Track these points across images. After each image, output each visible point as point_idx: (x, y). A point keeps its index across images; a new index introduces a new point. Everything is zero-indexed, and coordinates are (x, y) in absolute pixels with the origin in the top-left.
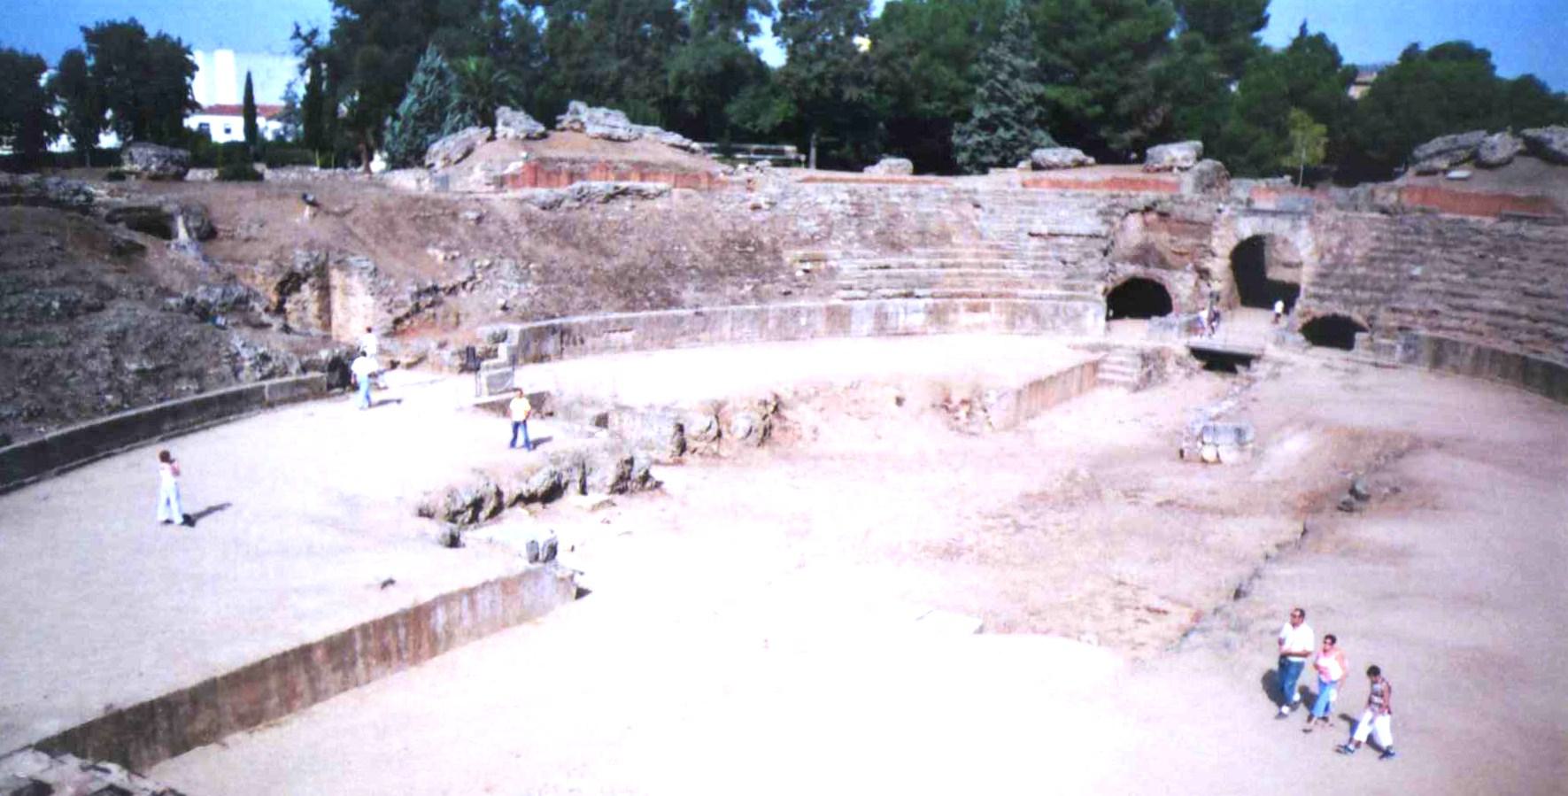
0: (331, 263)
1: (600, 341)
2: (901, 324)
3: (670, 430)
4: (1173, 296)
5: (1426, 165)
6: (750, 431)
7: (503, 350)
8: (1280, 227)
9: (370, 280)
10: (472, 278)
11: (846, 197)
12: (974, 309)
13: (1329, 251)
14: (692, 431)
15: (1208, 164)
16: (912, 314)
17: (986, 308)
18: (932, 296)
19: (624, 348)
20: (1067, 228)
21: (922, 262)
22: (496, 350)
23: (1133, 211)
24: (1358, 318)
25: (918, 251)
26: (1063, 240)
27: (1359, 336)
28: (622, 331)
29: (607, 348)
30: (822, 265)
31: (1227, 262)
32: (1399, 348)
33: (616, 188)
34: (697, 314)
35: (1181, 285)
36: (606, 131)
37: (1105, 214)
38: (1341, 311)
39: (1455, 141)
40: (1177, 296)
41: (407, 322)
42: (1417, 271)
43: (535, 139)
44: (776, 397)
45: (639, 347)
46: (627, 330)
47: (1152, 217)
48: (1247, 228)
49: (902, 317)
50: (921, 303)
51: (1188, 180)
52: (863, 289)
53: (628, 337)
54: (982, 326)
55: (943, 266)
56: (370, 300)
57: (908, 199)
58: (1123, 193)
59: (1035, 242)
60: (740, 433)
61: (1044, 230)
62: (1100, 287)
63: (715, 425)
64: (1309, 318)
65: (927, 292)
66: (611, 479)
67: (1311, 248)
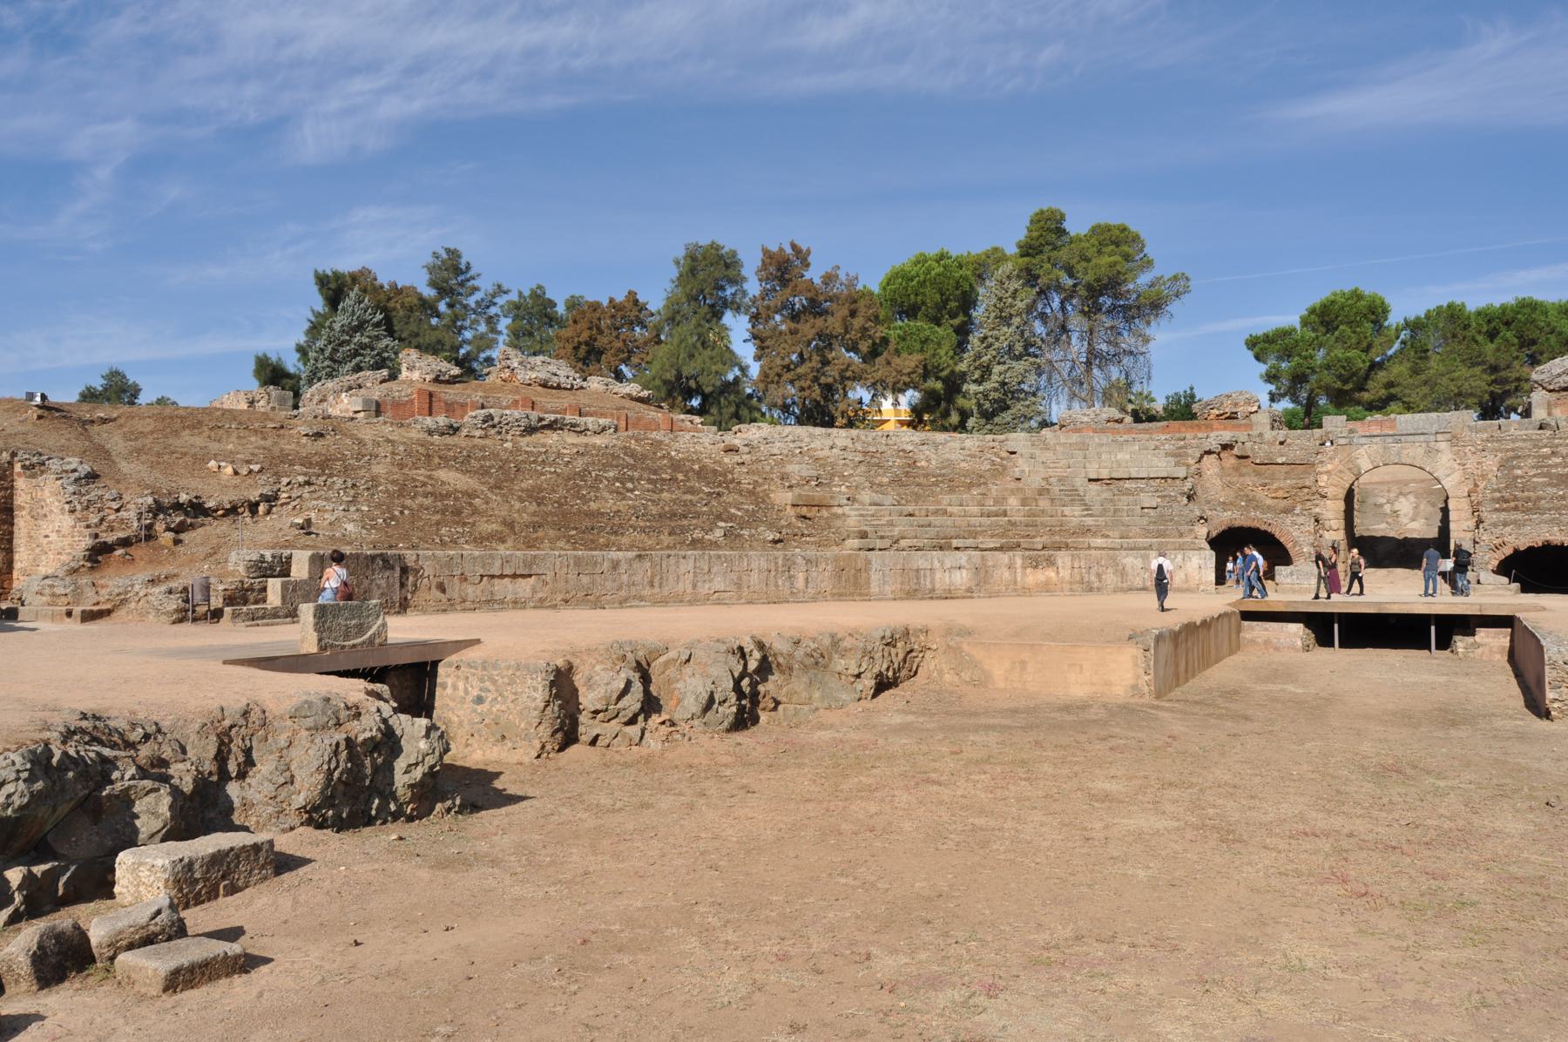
0: (18, 468)
1: (471, 591)
2: (937, 586)
3: (536, 692)
4: (1289, 546)
6: (711, 700)
9: (71, 489)
10: (271, 499)
13: (1483, 476)
14: (589, 699)
15: (1285, 404)
16: (953, 570)
17: (1051, 562)
18: (976, 548)
19: (517, 604)
21: (955, 509)
22: (264, 589)
23: (1209, 452)
25: (946, 499)
26: (1128, 484)
28: (515, 576)
29: (490, 603)
30: (825, 513)
33: (541, 419)
34: (640, 556)
35: (1294, 532)
36: (543, 375)
37: (1178, 455)
40: (1296, 543)
41: (119, 552)
43: (448, 382)
44: (761, 646)
45: (541, 604)
46: (523, 576)
47: (1229, 460)
49: (938, 575)
50: (962, 557)
51: (1263, 419)
52: (882, 537)
53: (524, 587)
54: (1046, 588)
56: (68, 520)
58: (1189, 436)
59: (1094, 487)
60: (692, 705)
61: (1104, 474)
62: (1202, 531)
63: (637, 687)
64: (1508, 551)
65: (969, 542)
66: (308, 787)
67: (1457, 476)
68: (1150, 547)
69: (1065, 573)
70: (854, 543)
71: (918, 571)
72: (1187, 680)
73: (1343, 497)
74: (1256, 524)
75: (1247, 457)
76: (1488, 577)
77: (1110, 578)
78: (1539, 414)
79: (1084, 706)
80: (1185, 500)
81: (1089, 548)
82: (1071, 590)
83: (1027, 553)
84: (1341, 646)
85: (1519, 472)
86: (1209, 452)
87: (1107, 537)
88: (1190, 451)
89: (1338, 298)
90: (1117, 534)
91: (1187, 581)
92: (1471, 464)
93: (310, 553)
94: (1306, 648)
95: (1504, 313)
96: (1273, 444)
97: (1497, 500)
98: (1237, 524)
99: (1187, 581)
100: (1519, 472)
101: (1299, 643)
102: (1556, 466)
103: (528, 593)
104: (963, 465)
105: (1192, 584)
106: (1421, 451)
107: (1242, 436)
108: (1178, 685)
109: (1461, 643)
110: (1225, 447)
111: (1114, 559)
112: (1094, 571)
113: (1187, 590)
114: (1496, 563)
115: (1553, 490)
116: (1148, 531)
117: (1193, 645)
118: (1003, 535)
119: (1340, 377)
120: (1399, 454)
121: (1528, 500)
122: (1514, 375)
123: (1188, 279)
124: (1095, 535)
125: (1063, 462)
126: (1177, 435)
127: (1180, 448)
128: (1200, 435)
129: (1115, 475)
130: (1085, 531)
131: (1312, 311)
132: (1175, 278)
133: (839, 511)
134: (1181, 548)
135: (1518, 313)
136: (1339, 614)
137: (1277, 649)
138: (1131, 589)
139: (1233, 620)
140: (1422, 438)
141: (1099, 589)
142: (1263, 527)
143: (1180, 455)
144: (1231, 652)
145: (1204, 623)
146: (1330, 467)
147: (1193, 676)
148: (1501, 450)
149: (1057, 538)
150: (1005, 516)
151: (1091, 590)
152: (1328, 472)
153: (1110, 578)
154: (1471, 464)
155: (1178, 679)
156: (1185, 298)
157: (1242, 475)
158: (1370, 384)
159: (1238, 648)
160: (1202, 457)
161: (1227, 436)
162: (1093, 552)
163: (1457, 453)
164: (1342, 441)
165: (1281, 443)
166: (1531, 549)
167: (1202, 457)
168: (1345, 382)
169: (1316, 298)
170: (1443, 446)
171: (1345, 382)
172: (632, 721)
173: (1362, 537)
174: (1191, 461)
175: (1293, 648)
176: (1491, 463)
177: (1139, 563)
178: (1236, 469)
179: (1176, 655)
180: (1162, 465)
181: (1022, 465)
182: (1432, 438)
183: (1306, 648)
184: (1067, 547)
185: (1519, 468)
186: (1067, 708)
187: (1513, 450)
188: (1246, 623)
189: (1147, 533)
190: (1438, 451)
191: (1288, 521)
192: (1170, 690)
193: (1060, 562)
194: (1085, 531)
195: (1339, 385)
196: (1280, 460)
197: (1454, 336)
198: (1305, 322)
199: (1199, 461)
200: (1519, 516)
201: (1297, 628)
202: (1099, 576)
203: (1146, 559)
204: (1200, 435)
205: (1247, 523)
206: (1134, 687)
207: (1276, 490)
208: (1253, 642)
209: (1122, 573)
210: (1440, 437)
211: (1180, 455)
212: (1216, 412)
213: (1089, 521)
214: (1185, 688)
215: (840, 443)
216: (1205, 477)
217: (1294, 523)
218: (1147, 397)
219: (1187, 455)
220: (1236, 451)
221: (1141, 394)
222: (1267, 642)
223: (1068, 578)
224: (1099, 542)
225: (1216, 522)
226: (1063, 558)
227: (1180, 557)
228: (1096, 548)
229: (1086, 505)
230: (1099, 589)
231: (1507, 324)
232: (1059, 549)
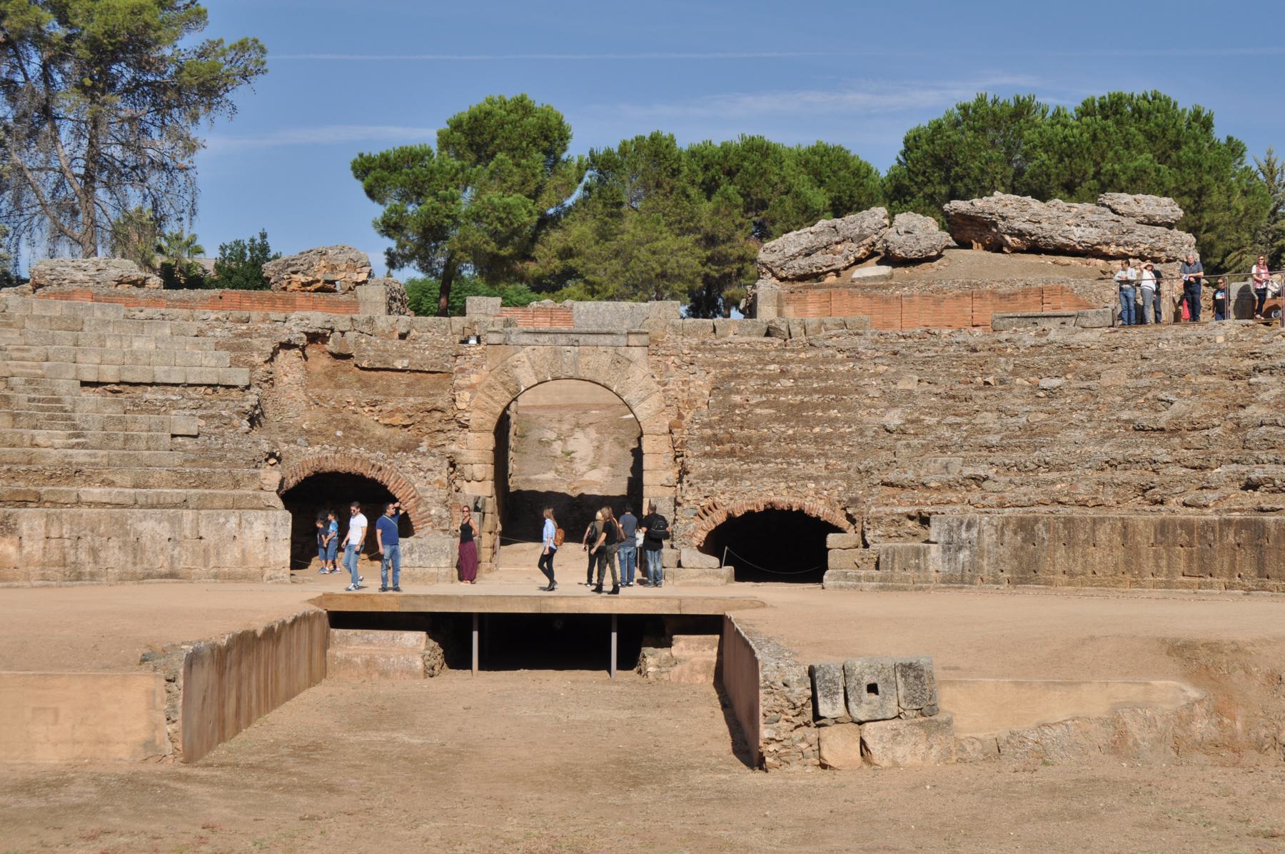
13: (691, 403)
15: (411, 273)
23: (287, 346)
24: (818, 508)
26: (150, 394)
27: (832, 539)
32: (935, 551)
37: (237, 348)
38: (784, 498)
40: (419, 501)
47: (320, 360)
51: (374, 296)
58: (255, 315)
59: (91, 395)
61: (110, 374)
62: (271, 477)
64: (720, 518)
67: (655, 402)
68: (184, 504)
69: (34, 548)
72: (238, 730)
74: (358, 468)
75: (349, 356)
76: (693, 557)
77: (114, 556)
78: (766, 312)
79: (59, 782)
80: (246, 425)
81: (78, 503)
82: (44, 577)
84: (481, 668)
85: (737, 399)
86: (287, 346)
87: (112, 484)
88: (256, 342)
89: (496, 108)
90: (128, 480)
91: (244, 561)
92: (674, 386)
94: (430, 672)
95: (725, 157)
96: (386, 336)
98: (329, 466)
99: (244, 561)
100: (737, 399)
101: (419, 664)
102: (786, 391)
105: (253, 568)
106: (606, 359)
107: (342, 322)
108: (222, 739)
109: (652, 657)
110: (315, 338)
111: (121, 523)
112: (84, 544)
113: (246, 577)
114: (702, 535)
115: (778, 428)
116: (182, 476)
117: (250, 668)
119: (494, 234)
120: (575, 362)
121: (748, 441)
122: (736, 252)
123: (263, 50)
124: (88, 480)
125: (36, 351)
126: (236, 314)
127: (241, 335)
128: (273, 316)
129: (128, 377)
130: (74, 473)
131: (457, 125)
132: (242, 46)
134: (236, 505)
135: (745, 159)
136: (481, 616)
137: (384, 674)
138: (149, 576)
139: (317, 627)
140: (608, 339)
141: (93, 576)
142: (371, 474)
143: (239, 348)
144: (313, 681)
145: (269, 632)
146: (474, 379)
147: (249, 723)
148: (714, 365)
149: (21, 485)
151: (79, 577)
152: (472, 387)
153: (114, 556)
154: (674, 386)
155: (223, 729)
156: (257, 81)
157: (339, 386)
158: (539, 250)
159: (324, 674)
160: (275, 353)
161: (317, 320)
162: (85, 510)
163: (655, 366)
164: (494, 339)
165: (403, 336)
166: (749, 514)
167: (275, 353)
168: (502, 243)
169: (465, 103)
170: (637, 353)
171: (502, 243)
173: (519, 492)
174: (258, 359)
175: (410, 672)
176: (701, 383)
177: (164, 530)
178: (330, 376)
179: (221, 689)
182: (622, 340)
183: (430, 672)
184: (39, 500)
185: (738, 392)
186: (27, 787)
187: (731, 365)
188: (337, 633)
189: (179, 479)
190: (630, 361)
191: (409, 465)
192: (210, 748)
193: (24, 527)
194: (74, 473)
195: (492, 247)
196: (399, 364)
197: (658, 185)
198: (445, 142)
199: (271, 360)
200: (735, 465)
201: (416, 640)
202: (94, 552)
203: (175, 522)
204: (273, 316)
205: (344, 466)
206: (149, 744)
207: (392, 413)
208: (347, 662)
209: (136, 548)
210: (633, 340)
211: (239, 348)
212: (300, 278)
213: (80, 456)
214: (233, 743)
216: (279, 386)
218: (188, 244)
219: (251, 349)
220: (330, 346)
221: (178, 238)
222: (370, 663)
223: (38, 555)
224: (95, 492)
225: (295, 462)
226: (30, 521)
227: (233, 521)
228: (90, 504)
229: (74, 427)
230: (93, 576)
231: (730, 173)
232: (25, 503)
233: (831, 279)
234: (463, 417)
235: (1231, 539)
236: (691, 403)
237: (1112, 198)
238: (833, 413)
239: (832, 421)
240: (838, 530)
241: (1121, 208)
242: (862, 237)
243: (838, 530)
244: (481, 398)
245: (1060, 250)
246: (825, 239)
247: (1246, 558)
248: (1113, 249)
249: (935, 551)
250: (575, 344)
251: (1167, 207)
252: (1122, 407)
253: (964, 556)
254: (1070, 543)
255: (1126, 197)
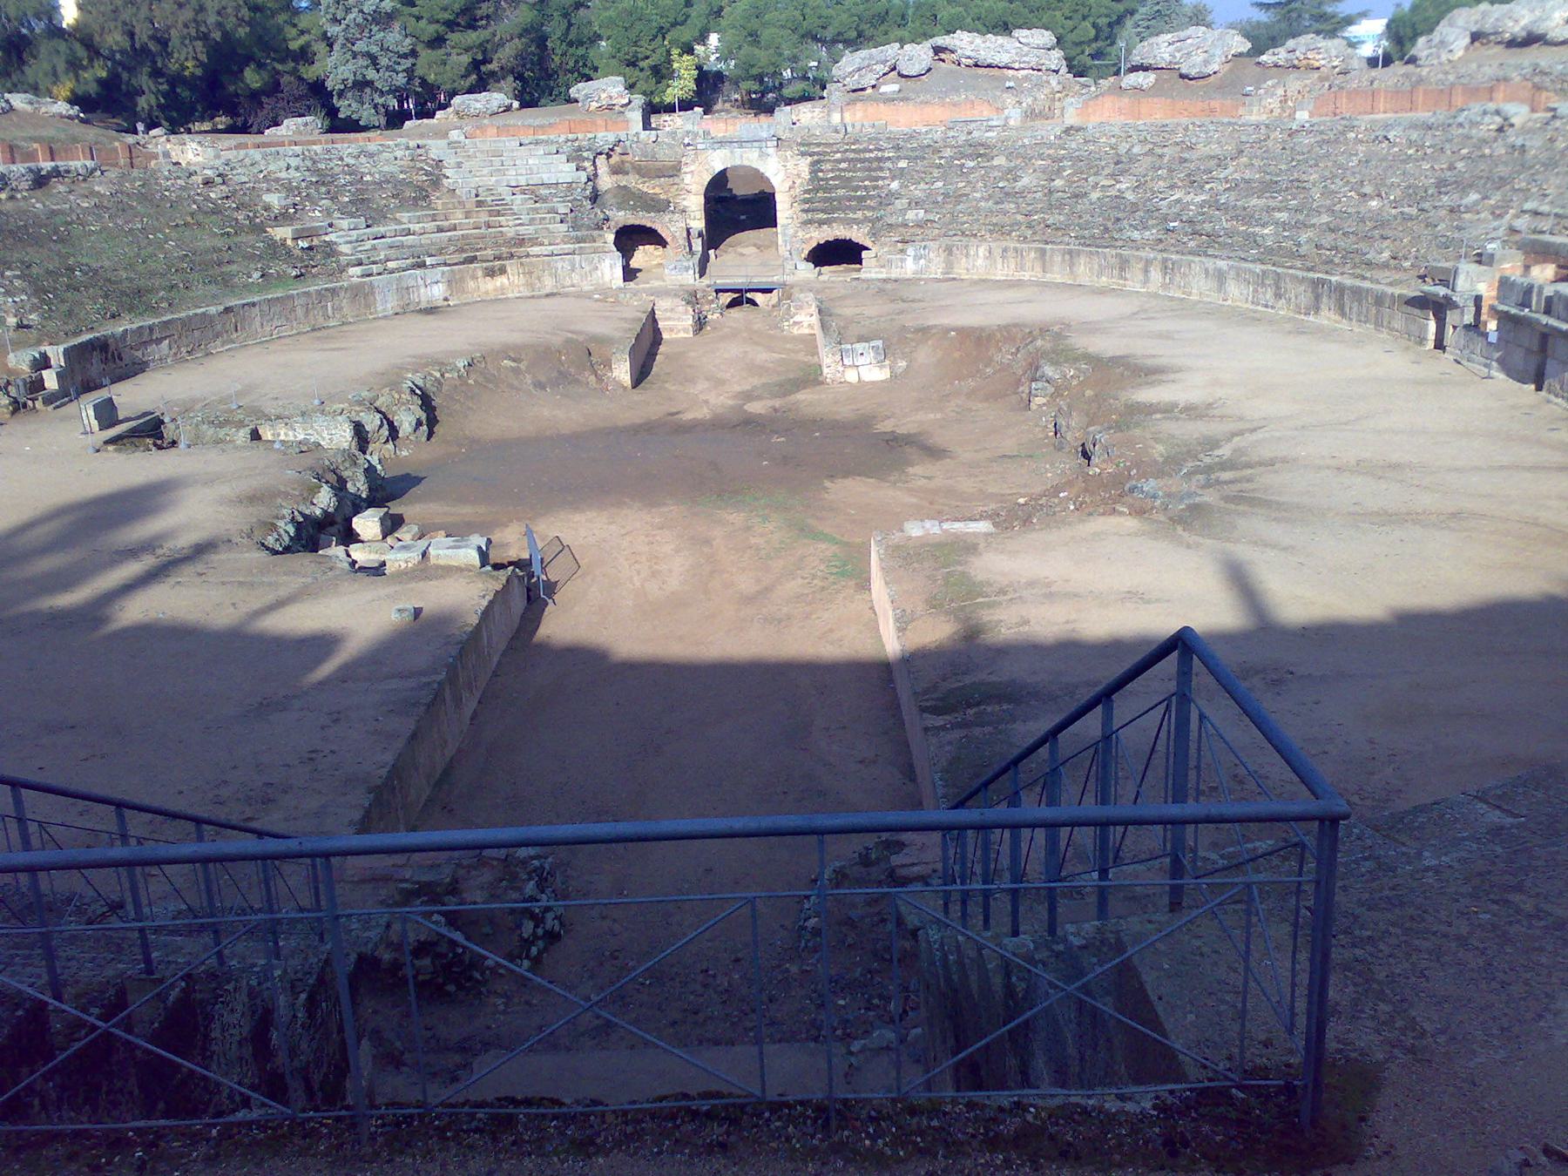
5: (851, 83)
7: (51, 380)
8: (749, 158)
11: (294, 162)
12: (491, 273)
17: (503, 271)
18: (445, 264)
20: (546, 178)
23: (601, 154)
24: (857, 235)
27: (864, 254)
31: (702, 200)
32: (910, 261)
35: (668, 226)
39: (871, 57)
42: (895, 185)
48: (718, 161)
49: (422, 290)
52: (374, 263)
55: (440, 230)
57: (363, 159)
64: (814, 245)
67: (781, 176)
70: (357, 270)
71: (407, 288)
73: (703, 191)
81: (528, 256)
83: (485, 265)
93: (61, 349)
97: (806, 201)
98: (630, 222)
103: (166, 351)
104: (402, 176)
118: (462, 250)
133: (327, 238)
140: (755, 144)
142: (649, 225)
146: (692, 168)
150: (455, 230)
154: (790, 165)
160: (594, 162)
170: (771, 151)
172: (387, 441)
180: (564, 171)
181: (452, 176)
187: (818, 154)
205: (637, 222)
210: (769, 144)
212: (594, 105)
215: (294, 162)
217: (670, 221)
224: (535, 250)
226: (511, 266)
233: (869, 91)
234: (689, 188)
235: (1033, 255)
236: (799, 176)
237: (1016, 33)
238: (867, 183)
239: (866, 188)
240: (867, 249)
241: (1022, 40)
242: (884, 62)
243: (867, 249)
244: (696, 179)
245: (989, 66)
246: (866, 63)
247: (1038, 265)
248: (1016, 66)
249: (910, 261)
250: (741, 147)
251: (1047, 37)
252: (1001, 179)
253: (922, 262)
254: (967, 255)
255: (1025, 32)
